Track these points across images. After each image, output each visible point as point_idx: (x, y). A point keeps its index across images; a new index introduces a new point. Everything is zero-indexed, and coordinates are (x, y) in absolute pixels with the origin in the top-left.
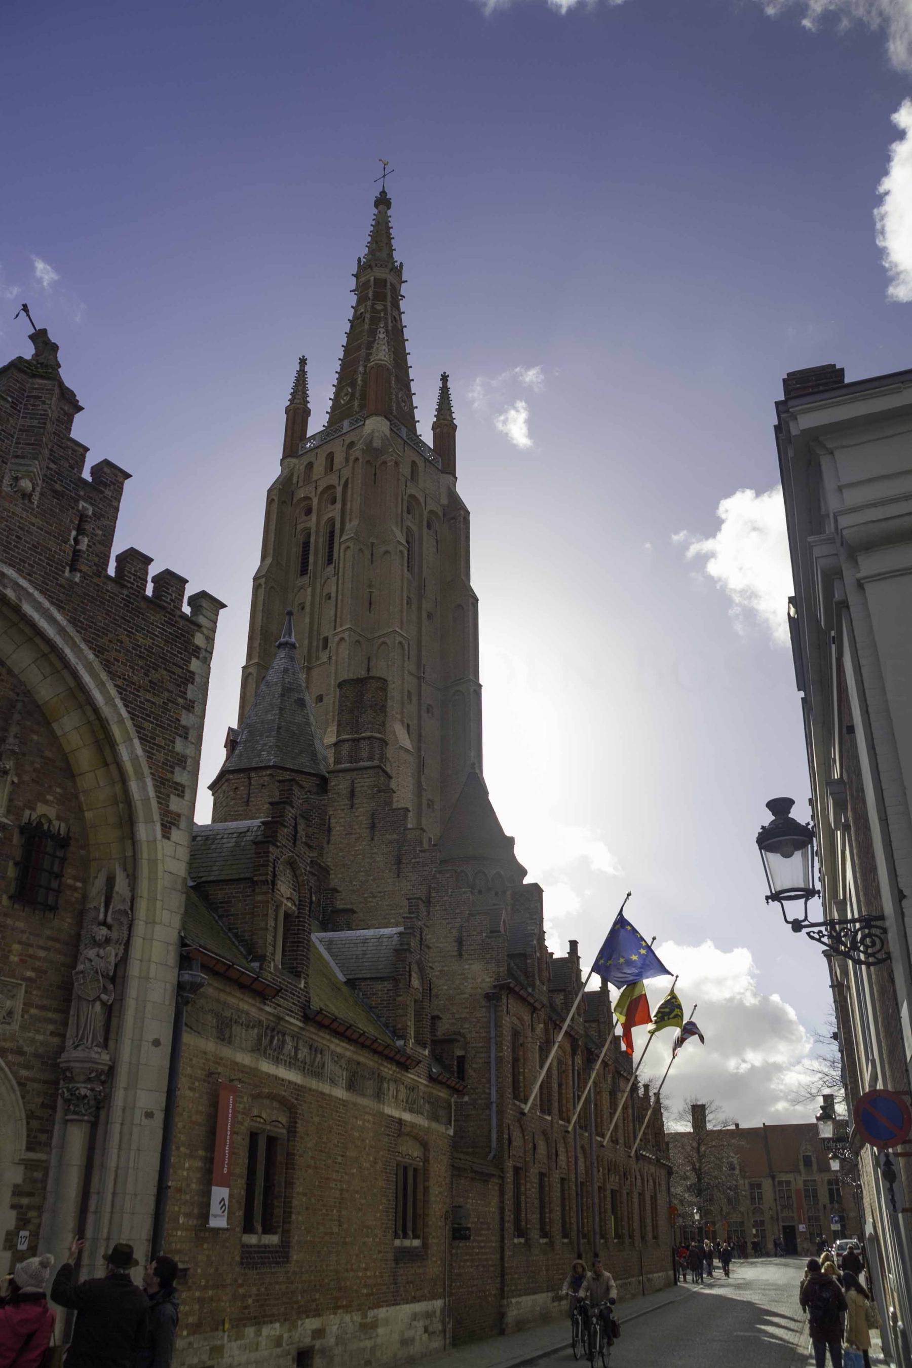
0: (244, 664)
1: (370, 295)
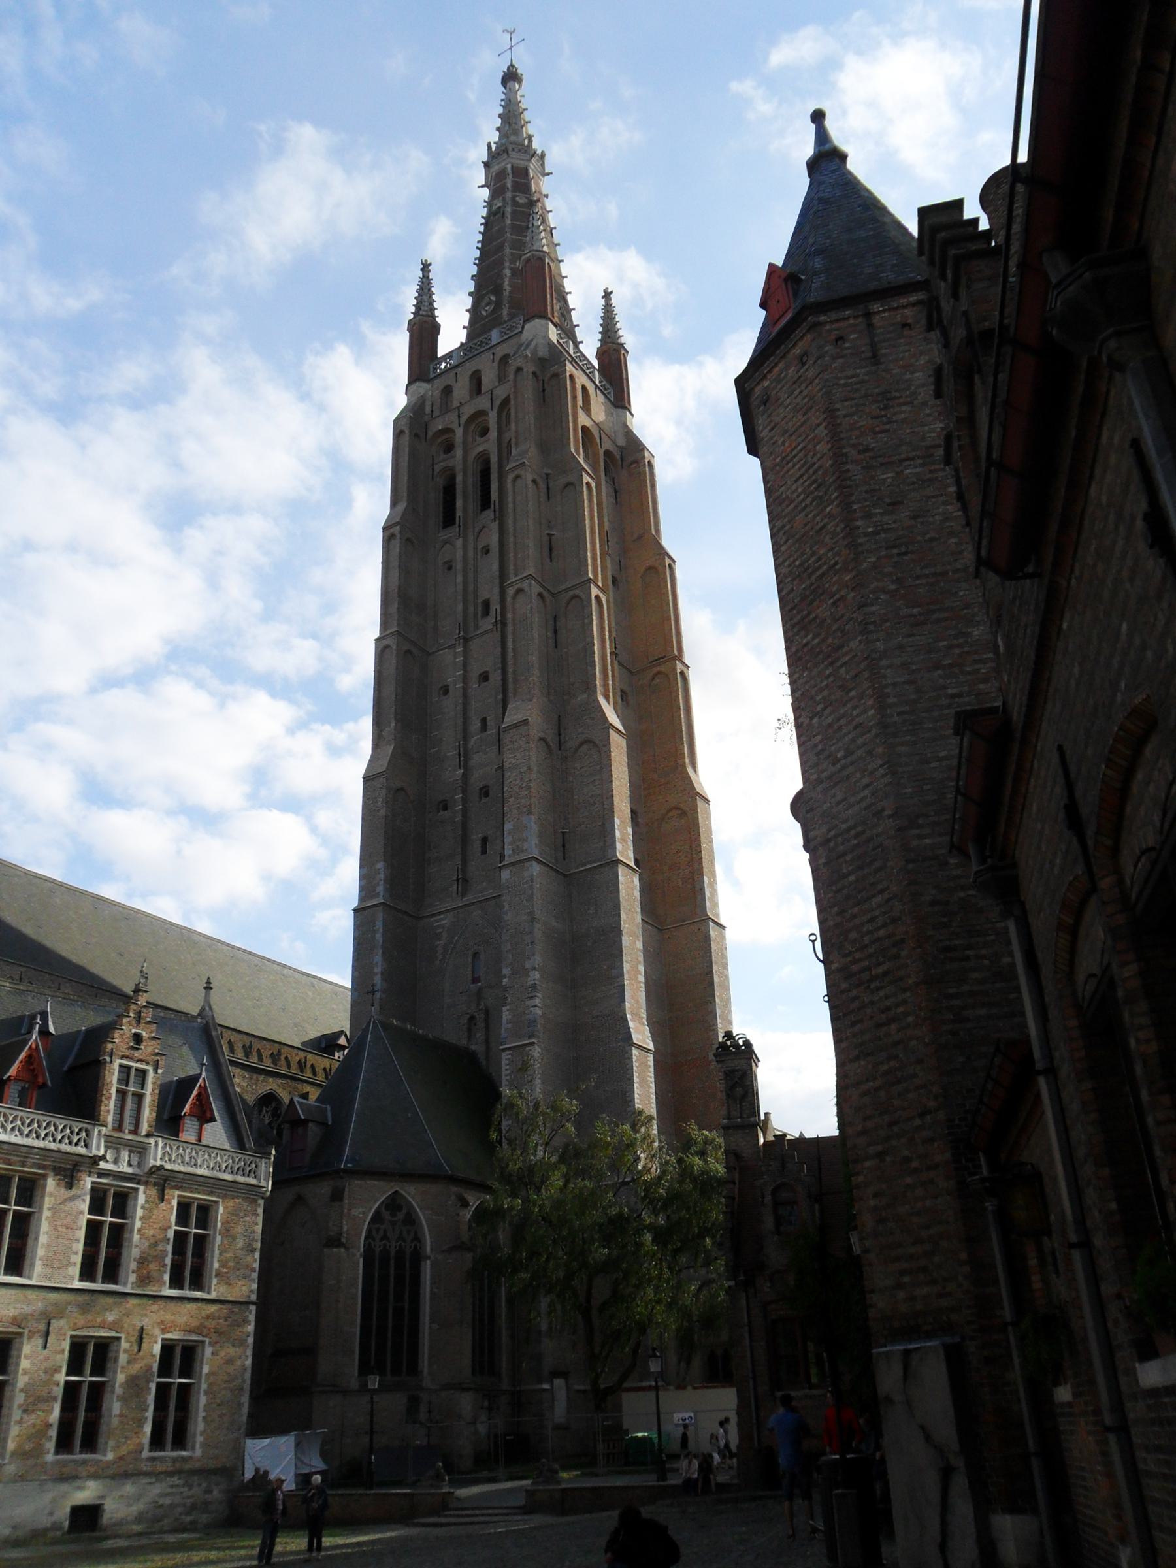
0: (377, 635)
1: (509, 185)
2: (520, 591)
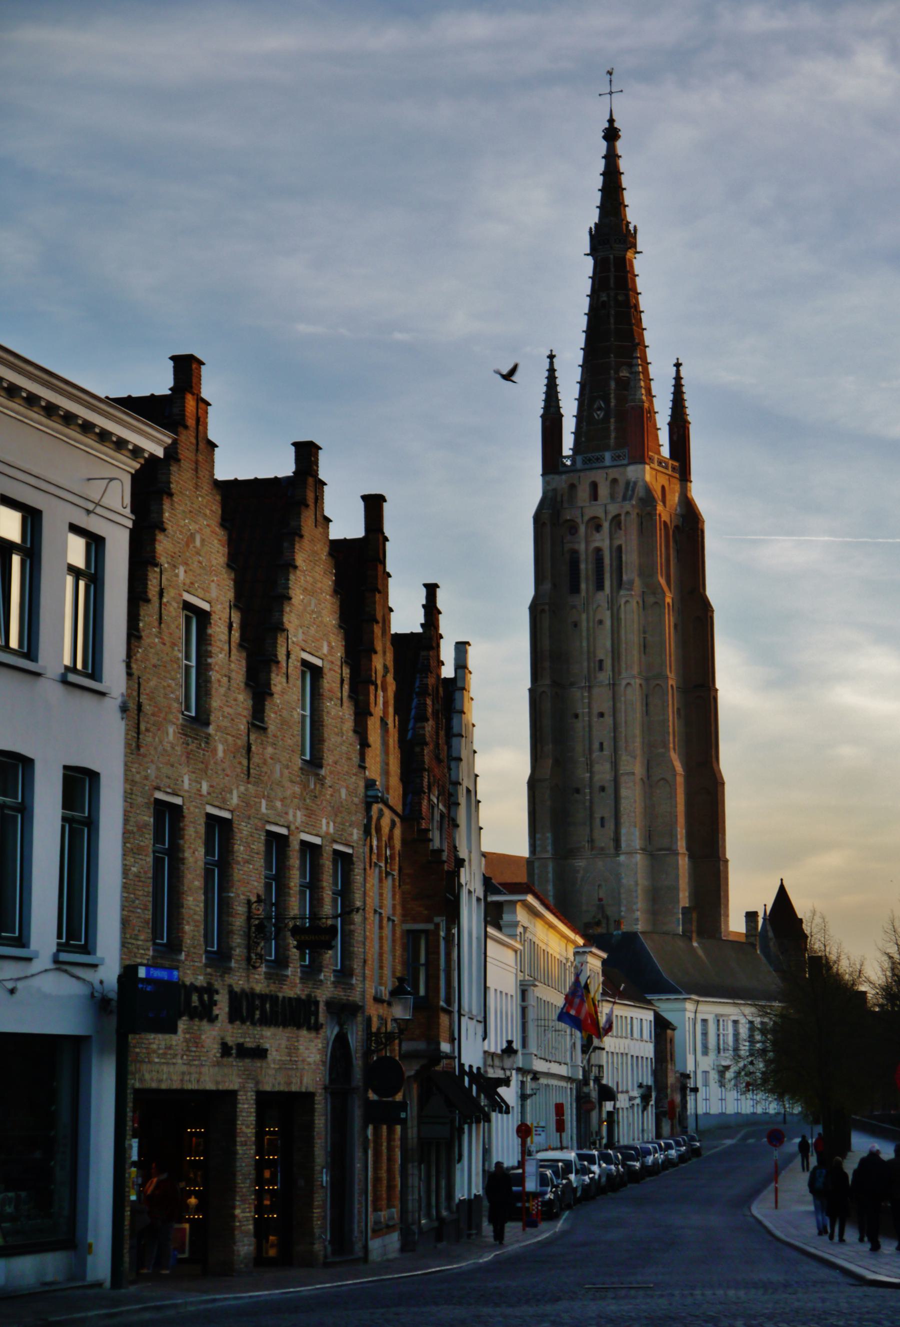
2: (628, 684)
